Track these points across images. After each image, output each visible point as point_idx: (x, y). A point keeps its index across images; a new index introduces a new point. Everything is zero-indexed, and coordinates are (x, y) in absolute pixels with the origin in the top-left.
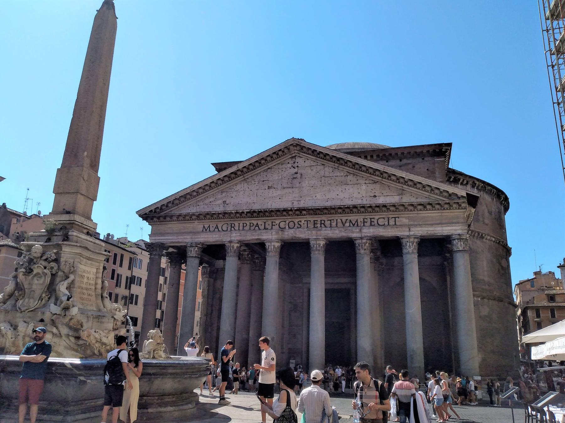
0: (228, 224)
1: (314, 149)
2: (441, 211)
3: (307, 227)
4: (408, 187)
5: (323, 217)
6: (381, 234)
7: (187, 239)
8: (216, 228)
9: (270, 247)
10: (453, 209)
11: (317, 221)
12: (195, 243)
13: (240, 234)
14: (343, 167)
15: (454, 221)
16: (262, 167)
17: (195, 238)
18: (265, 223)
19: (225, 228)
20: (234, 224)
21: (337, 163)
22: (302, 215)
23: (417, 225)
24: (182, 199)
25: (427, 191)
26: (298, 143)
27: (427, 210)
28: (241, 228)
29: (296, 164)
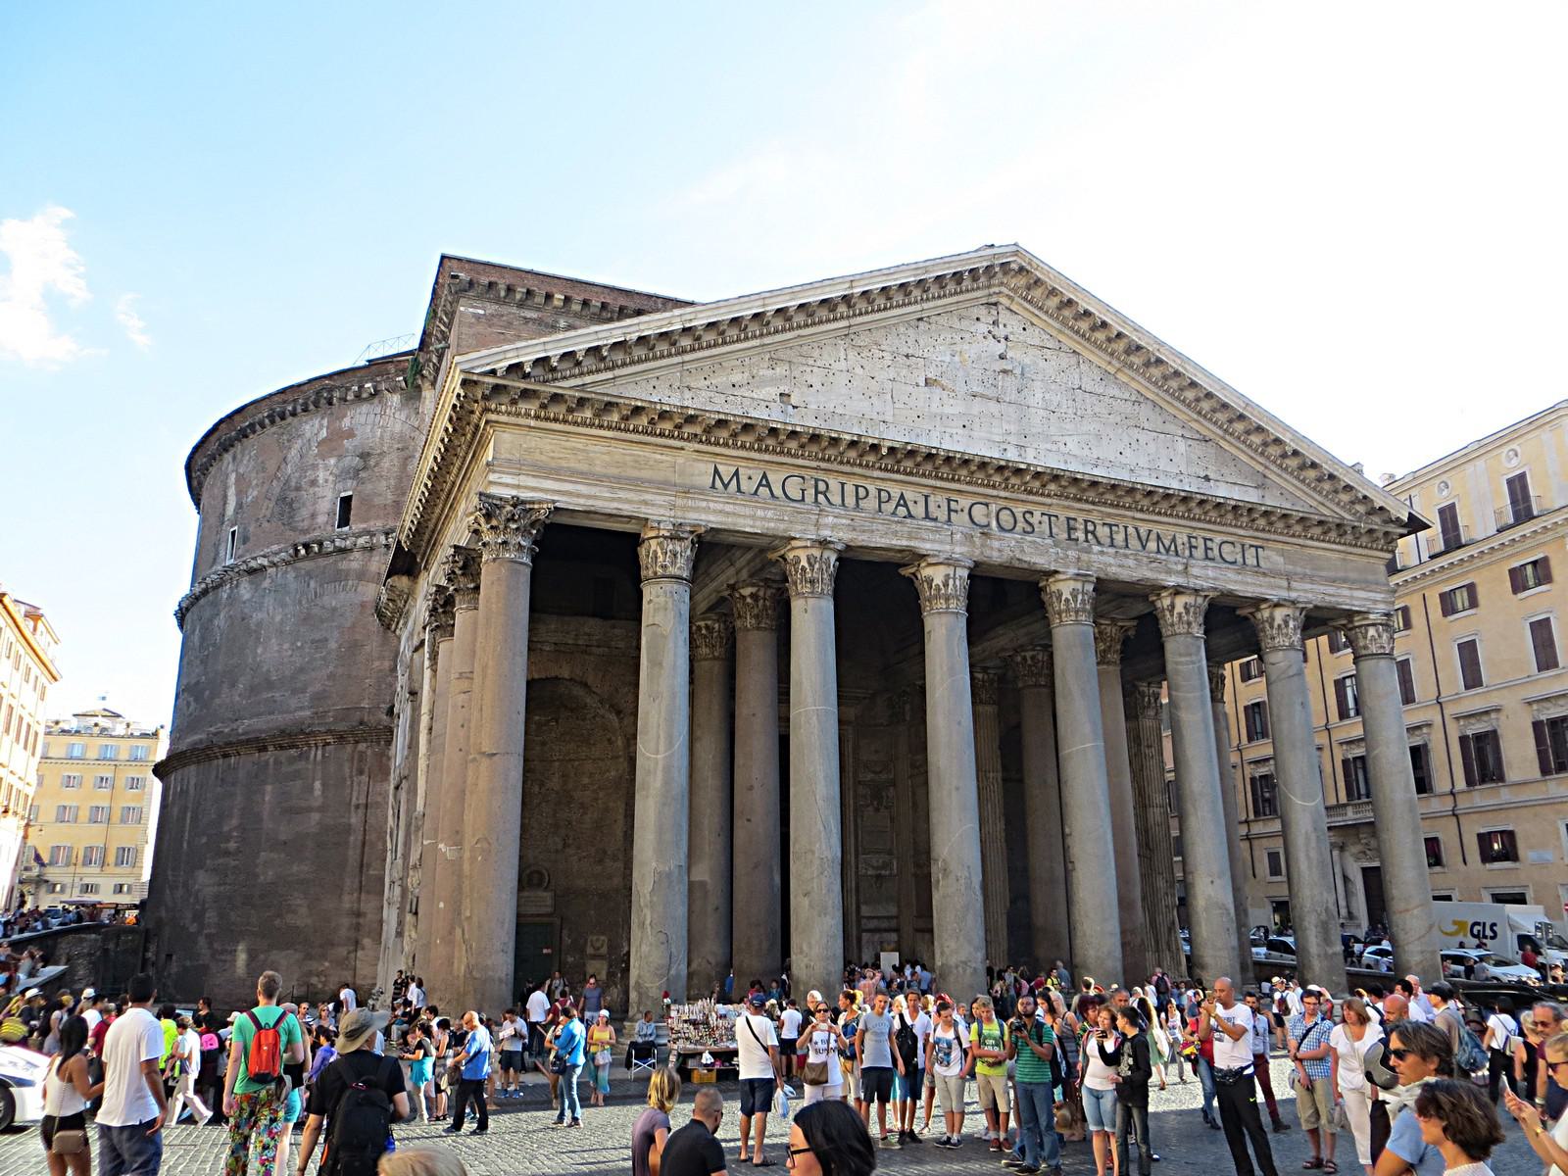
0: (803, 478)
1: (1072, 297)
2: (1350, 549)
3: (1051, 535)
4: (1279, 471)
5: (1095, 513)
6: (1231, 587)
7: (653, 505)
8: (760, 485)
9: (951, 582)
10: (1371, 548)
11: (1075, 519)
12: (688, 529)
14: (1133, 374)
15: (1370, 577)
17: (685, 508)
18: (926, 497)
22: (1042, 495)
23: (1305, 575)
24: (640, 352)
25: (1320, 493)
26: (1029, 268)
27: (1323, 541)
28: (850, 501)
29: (1000, 332)
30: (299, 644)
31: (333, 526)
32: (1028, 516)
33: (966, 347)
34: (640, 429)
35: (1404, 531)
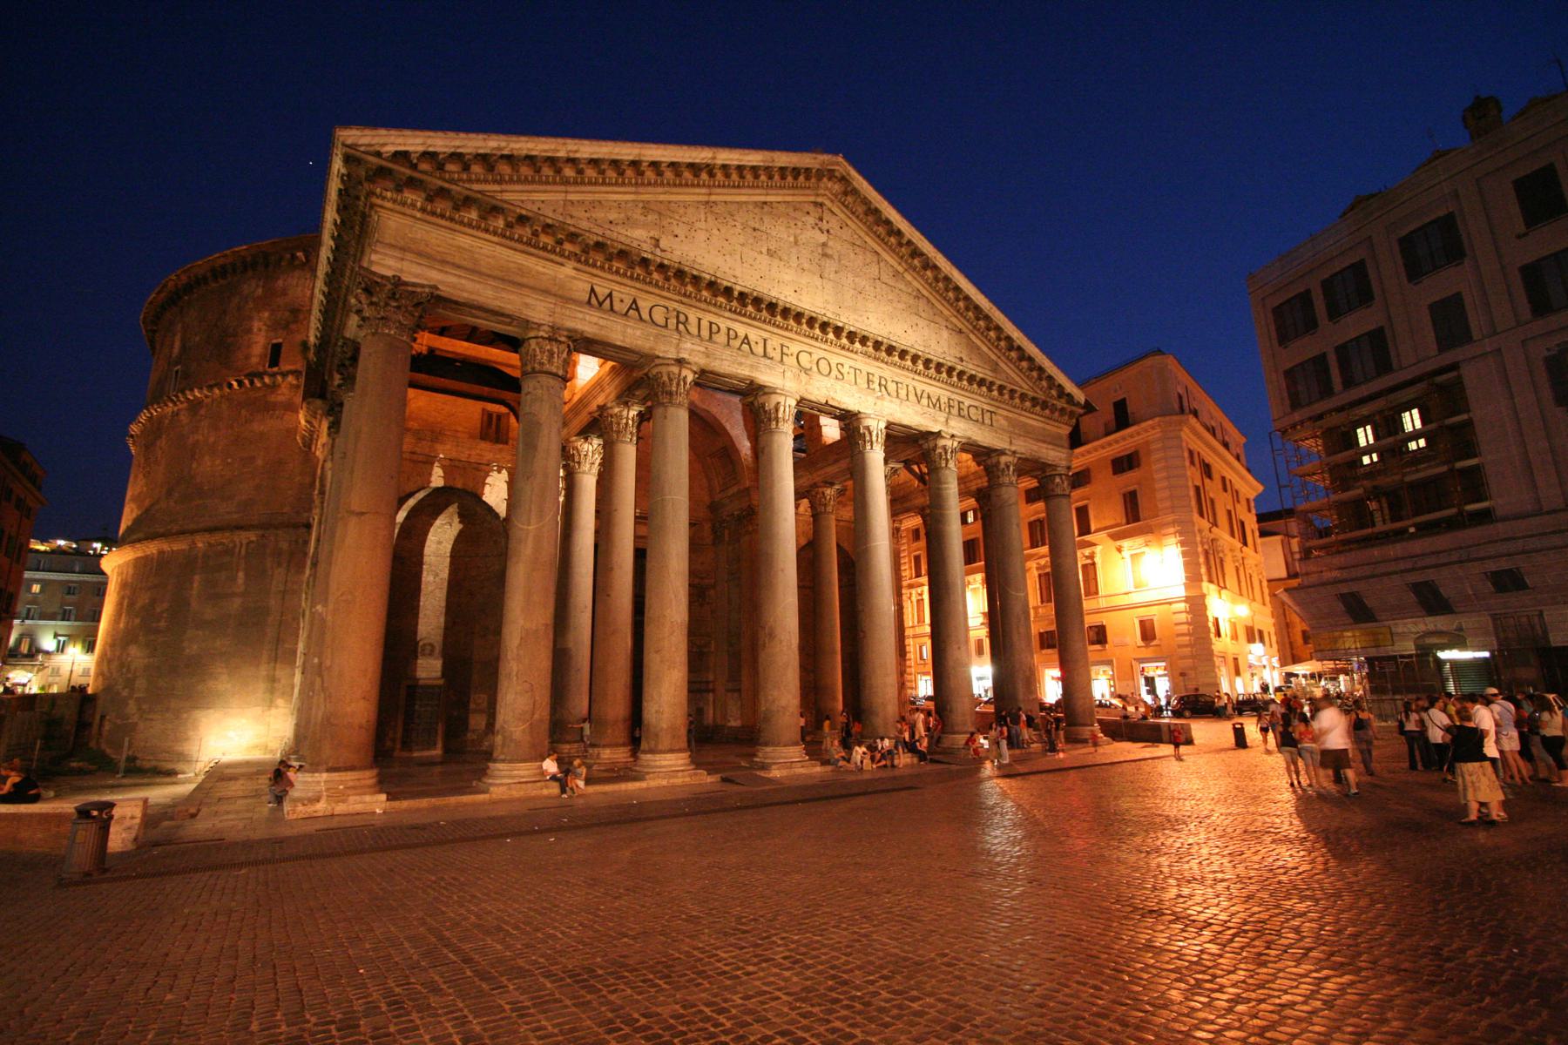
1: (878, 206)
2: (1048, 421)
5: (888, 372)
8: (630, 308)
9: (782, 409)
12: (565, 333)
13: (703, 349)
14: (916, 276)
16: (758, 191)
18: (765, 340)
19: (659, 316)
20: (687, 318)
21: (906, 261)
24: (525, 170)
27: (1032, 413)
28: (705, 333)
29: (825, 226)
30: (229, 460)
31: (264, 366)
32: (840, 366)
33: (799, 231)
34: (525, 239)
35: (1082, 411)
